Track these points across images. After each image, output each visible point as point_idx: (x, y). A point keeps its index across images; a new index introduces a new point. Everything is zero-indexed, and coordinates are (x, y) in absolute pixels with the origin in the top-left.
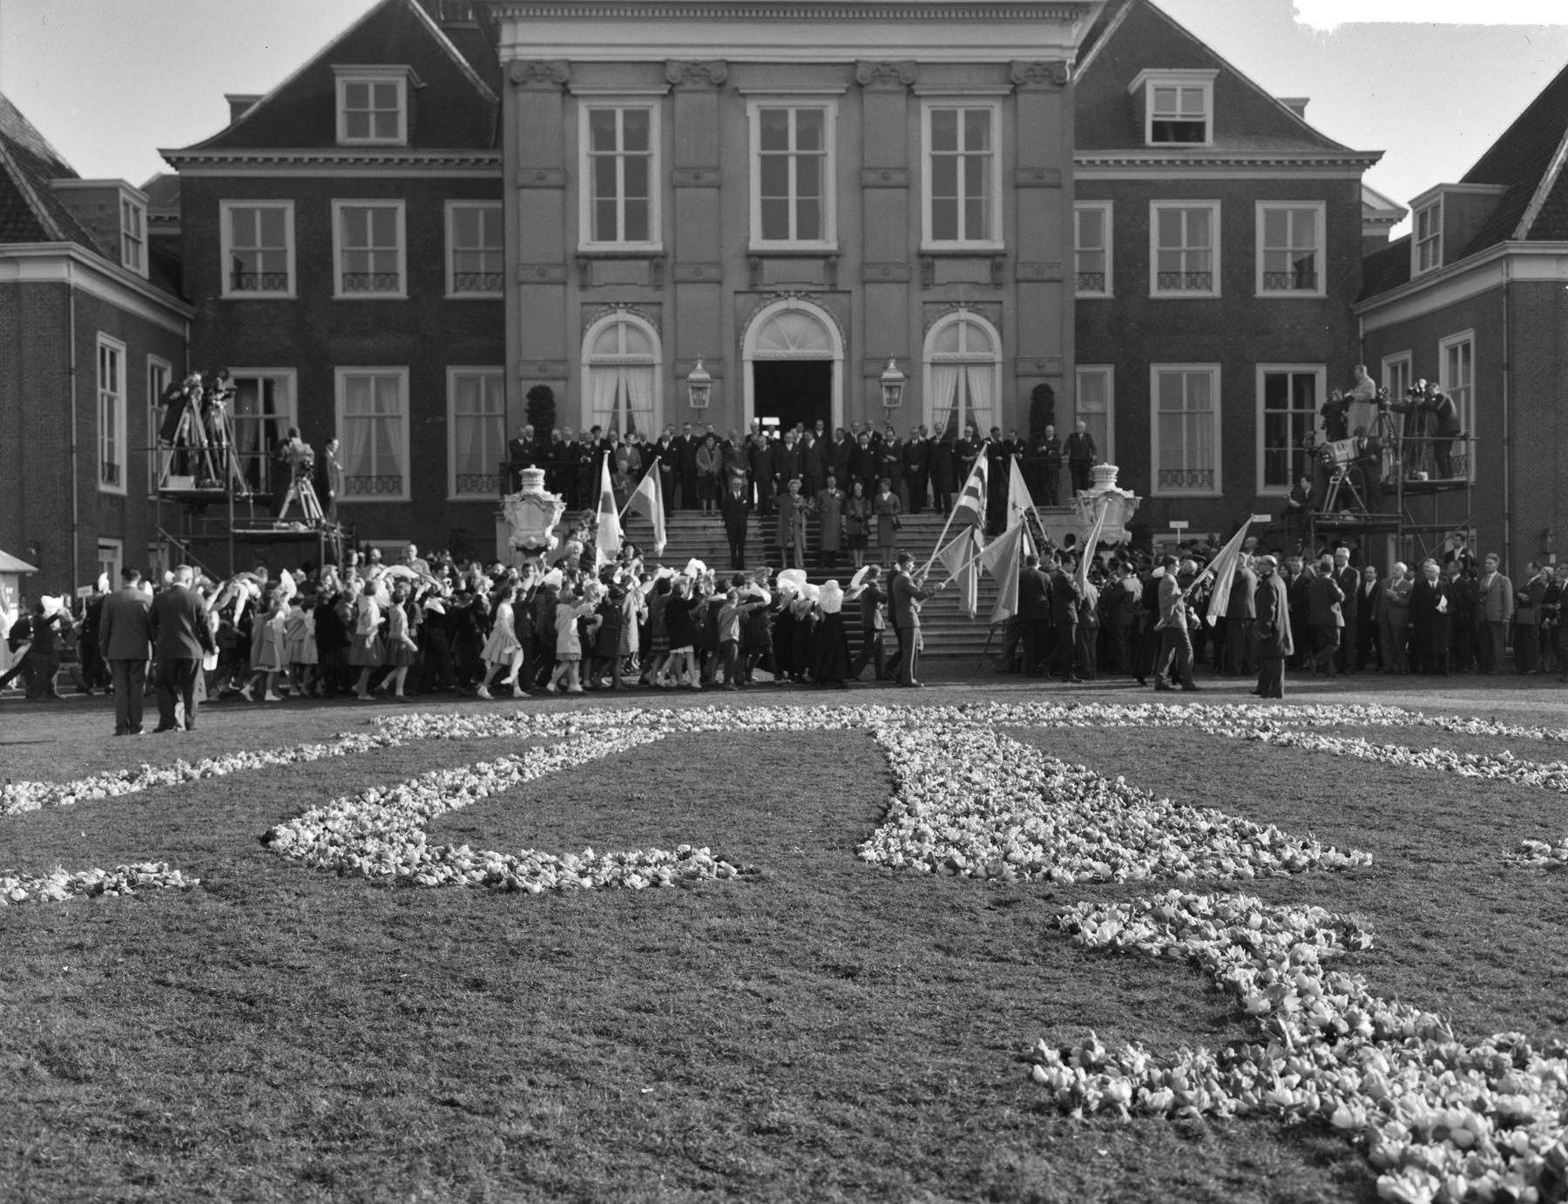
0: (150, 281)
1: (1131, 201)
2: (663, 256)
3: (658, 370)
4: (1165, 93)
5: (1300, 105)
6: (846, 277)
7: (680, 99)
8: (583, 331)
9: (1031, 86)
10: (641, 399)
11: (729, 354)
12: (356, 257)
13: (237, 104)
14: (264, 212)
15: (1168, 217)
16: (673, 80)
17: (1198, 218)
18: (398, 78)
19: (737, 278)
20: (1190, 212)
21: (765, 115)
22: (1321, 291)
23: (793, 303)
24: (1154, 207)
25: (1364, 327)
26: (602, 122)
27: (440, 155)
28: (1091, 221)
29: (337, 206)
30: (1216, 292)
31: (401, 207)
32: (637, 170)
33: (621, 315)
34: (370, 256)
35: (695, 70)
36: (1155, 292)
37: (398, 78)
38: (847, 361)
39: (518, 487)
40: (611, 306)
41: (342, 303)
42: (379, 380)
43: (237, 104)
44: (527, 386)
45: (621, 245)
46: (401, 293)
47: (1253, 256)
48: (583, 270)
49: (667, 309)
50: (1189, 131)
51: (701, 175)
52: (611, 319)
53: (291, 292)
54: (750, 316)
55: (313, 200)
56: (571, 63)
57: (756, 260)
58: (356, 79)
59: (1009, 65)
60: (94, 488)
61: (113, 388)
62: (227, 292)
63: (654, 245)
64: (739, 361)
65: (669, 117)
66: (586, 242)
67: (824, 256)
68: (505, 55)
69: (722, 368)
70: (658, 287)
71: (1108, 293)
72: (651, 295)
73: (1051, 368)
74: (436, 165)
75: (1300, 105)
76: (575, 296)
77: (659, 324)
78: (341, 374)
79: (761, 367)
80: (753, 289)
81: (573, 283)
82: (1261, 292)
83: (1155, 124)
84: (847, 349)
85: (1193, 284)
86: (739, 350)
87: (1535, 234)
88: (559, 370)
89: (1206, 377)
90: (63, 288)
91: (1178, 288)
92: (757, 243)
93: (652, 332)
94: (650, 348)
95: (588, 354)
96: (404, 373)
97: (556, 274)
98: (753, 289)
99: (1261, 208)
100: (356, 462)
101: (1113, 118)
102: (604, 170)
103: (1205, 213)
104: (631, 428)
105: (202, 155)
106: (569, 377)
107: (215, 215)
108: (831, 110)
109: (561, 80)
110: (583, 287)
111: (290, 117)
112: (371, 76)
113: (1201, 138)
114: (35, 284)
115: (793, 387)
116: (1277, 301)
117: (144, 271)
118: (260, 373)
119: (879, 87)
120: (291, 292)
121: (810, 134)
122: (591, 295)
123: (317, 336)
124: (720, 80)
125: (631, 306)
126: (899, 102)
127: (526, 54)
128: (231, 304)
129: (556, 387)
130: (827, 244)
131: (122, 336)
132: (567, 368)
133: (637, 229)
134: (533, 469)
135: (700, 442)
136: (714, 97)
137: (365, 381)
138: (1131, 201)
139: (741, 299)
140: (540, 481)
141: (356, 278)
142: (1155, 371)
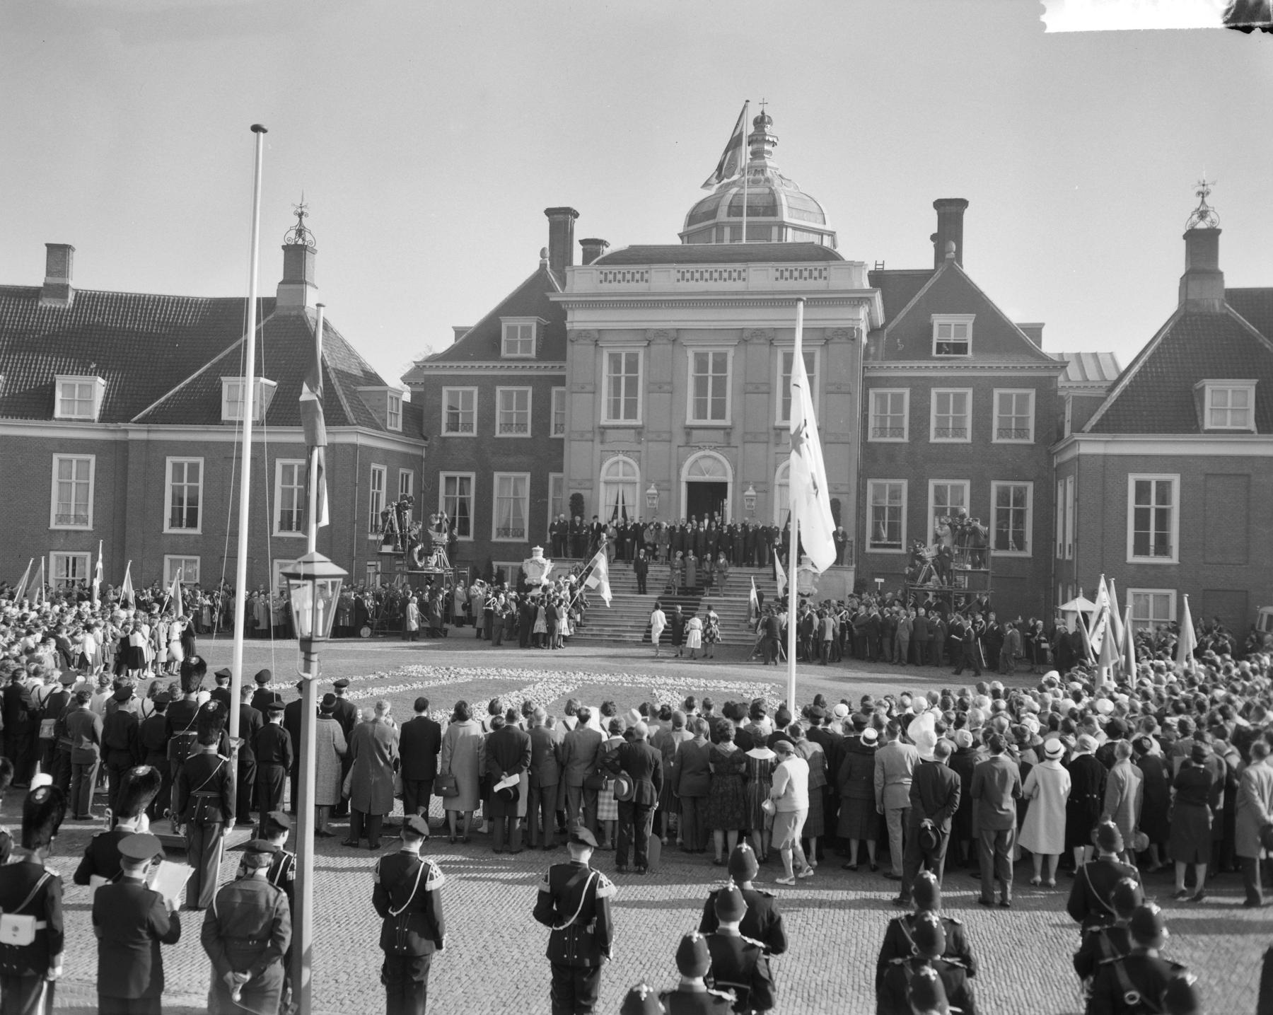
0: (404, 433)
1: (920, 388)
2: (642, 427)
3: (638, 486)
4: (945, 328)
5: (1035, 331)
6: (736, 439)
7: (654, 348)
8: (601, 465)
9: (836, 340)
10: (629, 501)
11: (674, 479)
12: (508, 416)
13: (459, 332)
14: (464, 392)
15: (943, 399)
16: (649, 338)
17: (960, 399)
18: (532, 323)
19: (680, 439)
20: (956, 395)
21: (696, 354)
22: (1031, 440)
23: (707, 452)
24: (934, 392)
25: (1056, 461)
26: (615, 359)
27: (550, 365)
28: (898, 399)
29: (499, 389)
30: (969, 440)
31: (530, 390)
32: (632, 385)
33: (621, 457)
34: (512, 415)
35: (662, 333)
36: (933, 440)
37: (532, 323)
38: (734, 482)
39: (530, 556)
40: (615, 452)
41: (499, 439)
42: (516, 479)
43: (459, 332)
44: (573, 492)
45: (622, 421)
46: (528, 434)
47: (991, 419)
48: (602, 434)
49: (643, 454)
50: (960, 348)
51: (666, 387)
52: (615, 459)
53: (474, 434)
54: (685, 459)
55: (487, 386)
56: (599, 331)
57: (689, 429)
58: (511, 324)
59: (824, 329)
60: (366, 539)
61: (379, 488)
62: (444, 433)
63: (638, 422)
64: (679, 482)
65: (648, 356)
66: (604, 420)
67: (724, 428)
68: (568, 326)
69: (666, 486)
70: (640, 443)
71: (906, 439)
72: (636, 447)
73: (844, 489)
74: (546, 369)
75: (1035, 331)
76: (598, 447)
77: (639, 461)
78: (497, 476)
79: (692, 486)
80: (687, 444)
81: (598, 439)
82: (995, 440)
83: (939, 345)
84: (735, 476)
85: (956, 435)
86: (679, 475)
87: (1095, 430)
88: (588, 484)
89: (962, 487)
90: (354, 446)
91: (947, 436)
92: (691, 420)
93: (637, 468)
94: (634, 474)
95: (603, 476)
96: (528, 476)
97: (589, 436)
98: (687, 444)
99: (997, 393)
100: (504, 521)
101: (916, 342)
102: (617, 382)
103: (964, 395)
104: (624, 515)
105: (434, 365)
106: (593, 487)
107: (440, 393)
108: (731, 353)
109: (596, 339)
110: (602, 442)
111: (481, 342)
112: (519, 322)
113: (966, 353)
114: (342, 444)
115: (706, 496)
116: (1004, 445)
117: (400, 429)
118: (458, 474)
119: (755, 341)
120: (474, 434)
121: (720, 365)
122: (606, 447)
123: (488, 455)
124: (675, 338)
125: (626, 453)
126: (766, 349)
127: (578, 326)
128: (445, 438)
129: (582, 492)
130: (727, 422)
131: (385, 463)
132: (592, 483)
133: (631, 413)
134: (538, 548)
135: (646, 526)
136: (670, 347)
137: (509, 479)
138: (920, 388)
139: (681, 449)
140: (541, 553)
141: (507, 426)
142: (932, 483)
